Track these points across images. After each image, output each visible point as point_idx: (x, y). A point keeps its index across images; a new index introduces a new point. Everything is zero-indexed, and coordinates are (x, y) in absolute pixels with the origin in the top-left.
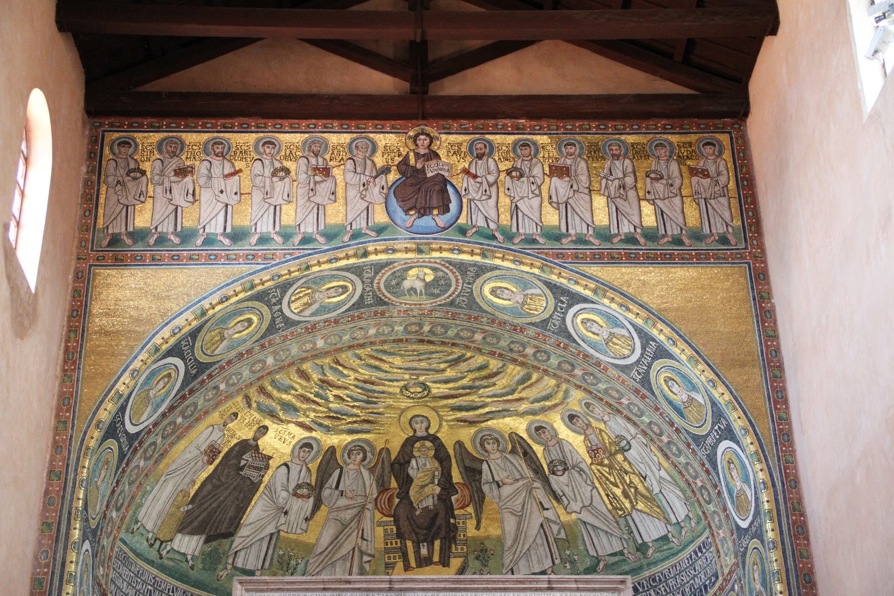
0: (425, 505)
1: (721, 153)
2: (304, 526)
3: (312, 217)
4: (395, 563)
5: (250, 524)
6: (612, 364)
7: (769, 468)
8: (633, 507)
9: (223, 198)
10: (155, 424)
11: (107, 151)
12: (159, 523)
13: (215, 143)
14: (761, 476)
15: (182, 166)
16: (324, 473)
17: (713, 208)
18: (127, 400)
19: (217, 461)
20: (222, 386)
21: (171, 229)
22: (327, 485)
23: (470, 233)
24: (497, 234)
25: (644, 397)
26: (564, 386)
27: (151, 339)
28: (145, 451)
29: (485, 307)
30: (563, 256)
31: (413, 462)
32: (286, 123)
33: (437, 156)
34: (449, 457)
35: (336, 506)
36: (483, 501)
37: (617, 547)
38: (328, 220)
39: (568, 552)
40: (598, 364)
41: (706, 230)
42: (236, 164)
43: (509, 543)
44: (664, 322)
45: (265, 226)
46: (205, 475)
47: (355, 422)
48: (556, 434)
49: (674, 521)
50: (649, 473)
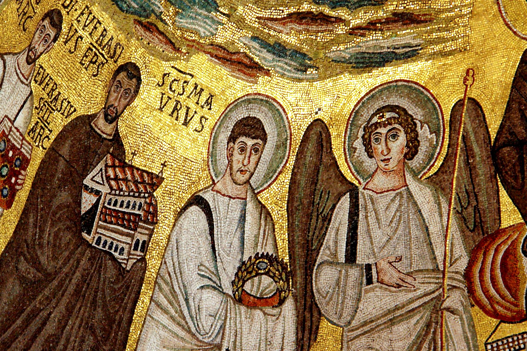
22: (323, 255)
35: (360, 318)
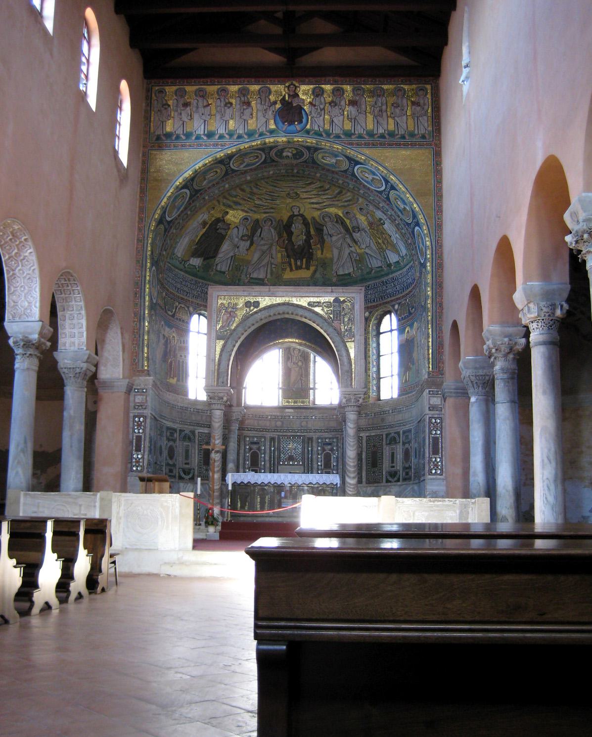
0: (299, 243)
1: (426, 95)
2: (246, 253)
3: (242, 127)
4: (286, 269)
5: (223, 252)
6: (375, 190)
7: (431, 240)
8: (386, 248)
9: (204, 117)
10: (179, 216)
11: (153, 95)
12: (183, 253)
13: (200, 91)
14: (428, 243)
15: (186, 102)
16: (254, 231)
17: (421, 122)
18: (166, 209)
19: (207, 227)
20: (207, 198)
21: (182, 132)
23: (311, 133)
24: (323, 134)
25: (388, 205)
26: (356, 197)
27: (175, 182)
28: (175, 226)
29: (320, 164)
30: (352, 144)
31: (294, 225)
32: (231, 80)
33: (298, 96)
34: (309, 224)
36: (324, 243)
37: (380, 265)
38: (249, 128)
39: (360, 265)
40: (369, 189)
41: (416, 132)
42: (209, 100)
43: (335, 260)
44: (393, 175)
45: (221, 131)
46: (201, 233)
47: (266, 209)
48: (354, 216)
49: (402, 255)
50: (392, 235)
